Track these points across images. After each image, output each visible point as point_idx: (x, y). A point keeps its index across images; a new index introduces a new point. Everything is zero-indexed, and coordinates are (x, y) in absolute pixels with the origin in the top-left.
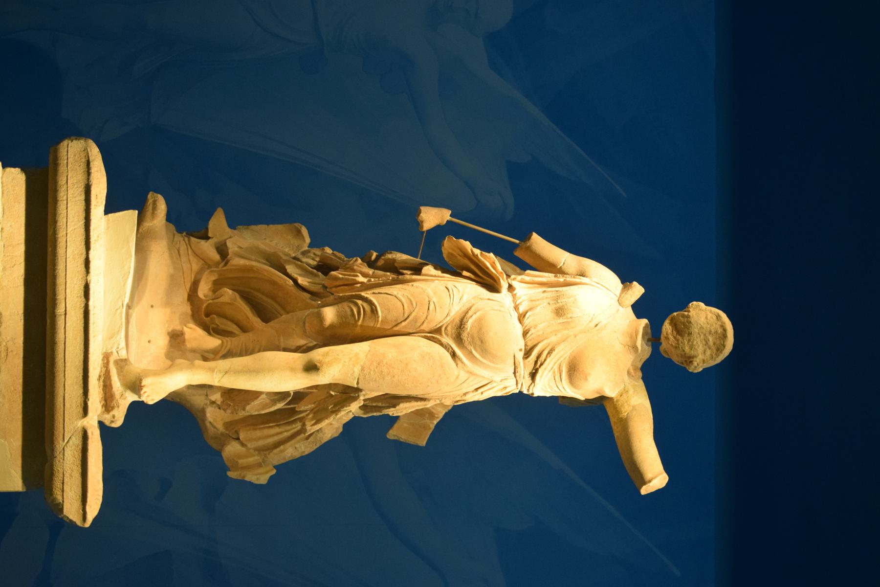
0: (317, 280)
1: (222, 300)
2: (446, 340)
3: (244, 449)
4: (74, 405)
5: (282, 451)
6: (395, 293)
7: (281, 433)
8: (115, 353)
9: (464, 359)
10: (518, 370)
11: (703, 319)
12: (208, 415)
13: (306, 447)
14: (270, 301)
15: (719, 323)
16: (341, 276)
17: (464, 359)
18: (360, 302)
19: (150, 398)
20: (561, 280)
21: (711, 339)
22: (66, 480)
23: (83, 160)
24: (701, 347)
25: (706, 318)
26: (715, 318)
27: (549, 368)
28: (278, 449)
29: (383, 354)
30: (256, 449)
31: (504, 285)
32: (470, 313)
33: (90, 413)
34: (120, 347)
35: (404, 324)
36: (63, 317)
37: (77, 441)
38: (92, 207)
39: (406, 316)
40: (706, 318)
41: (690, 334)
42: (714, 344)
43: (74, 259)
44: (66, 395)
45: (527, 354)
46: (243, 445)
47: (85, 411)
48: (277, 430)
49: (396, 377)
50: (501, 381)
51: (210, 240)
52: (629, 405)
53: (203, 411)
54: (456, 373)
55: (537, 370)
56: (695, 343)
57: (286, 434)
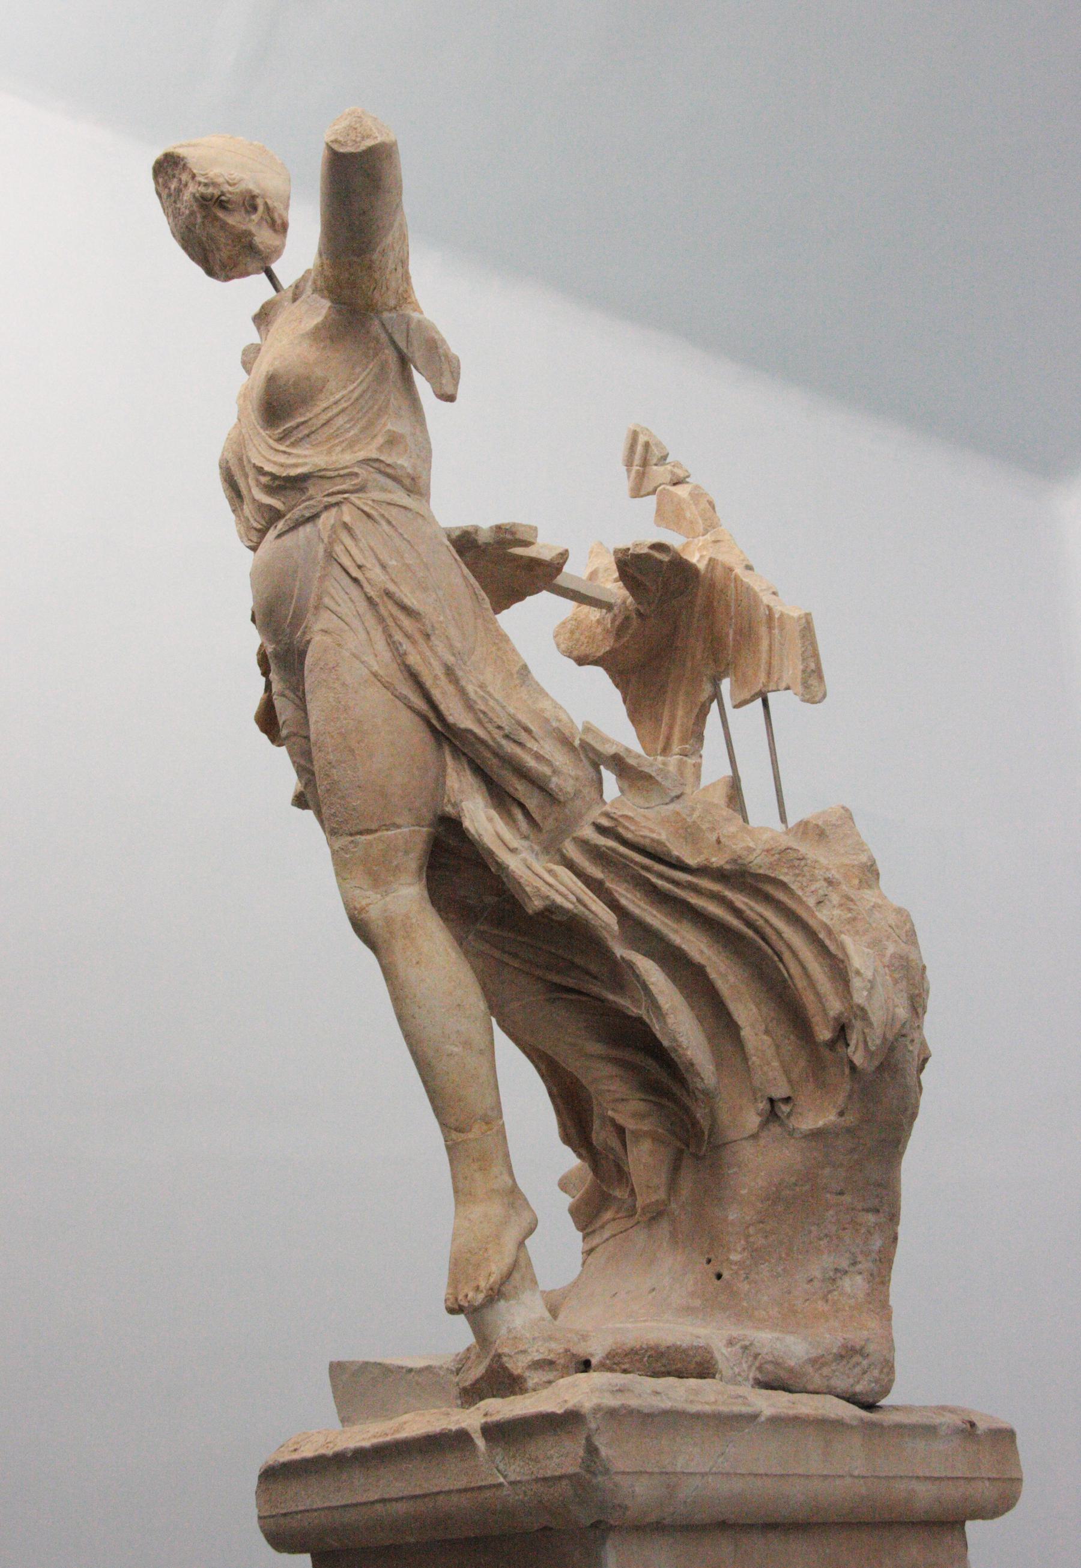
5: (830, 932)
7: (789, 947)
12: (821, 1123)
13: (813, 879)
19: (483, 1284)
27: (282, 459)
28: (827, 942)
33: (464, 1425)
42: (174, 176)
44: (459, 1485)
45: (275, 515)
47: (461, 1438)
48: (787, 956)
53: (816, 1135)
55: (288, 479)
57: (789, 932)
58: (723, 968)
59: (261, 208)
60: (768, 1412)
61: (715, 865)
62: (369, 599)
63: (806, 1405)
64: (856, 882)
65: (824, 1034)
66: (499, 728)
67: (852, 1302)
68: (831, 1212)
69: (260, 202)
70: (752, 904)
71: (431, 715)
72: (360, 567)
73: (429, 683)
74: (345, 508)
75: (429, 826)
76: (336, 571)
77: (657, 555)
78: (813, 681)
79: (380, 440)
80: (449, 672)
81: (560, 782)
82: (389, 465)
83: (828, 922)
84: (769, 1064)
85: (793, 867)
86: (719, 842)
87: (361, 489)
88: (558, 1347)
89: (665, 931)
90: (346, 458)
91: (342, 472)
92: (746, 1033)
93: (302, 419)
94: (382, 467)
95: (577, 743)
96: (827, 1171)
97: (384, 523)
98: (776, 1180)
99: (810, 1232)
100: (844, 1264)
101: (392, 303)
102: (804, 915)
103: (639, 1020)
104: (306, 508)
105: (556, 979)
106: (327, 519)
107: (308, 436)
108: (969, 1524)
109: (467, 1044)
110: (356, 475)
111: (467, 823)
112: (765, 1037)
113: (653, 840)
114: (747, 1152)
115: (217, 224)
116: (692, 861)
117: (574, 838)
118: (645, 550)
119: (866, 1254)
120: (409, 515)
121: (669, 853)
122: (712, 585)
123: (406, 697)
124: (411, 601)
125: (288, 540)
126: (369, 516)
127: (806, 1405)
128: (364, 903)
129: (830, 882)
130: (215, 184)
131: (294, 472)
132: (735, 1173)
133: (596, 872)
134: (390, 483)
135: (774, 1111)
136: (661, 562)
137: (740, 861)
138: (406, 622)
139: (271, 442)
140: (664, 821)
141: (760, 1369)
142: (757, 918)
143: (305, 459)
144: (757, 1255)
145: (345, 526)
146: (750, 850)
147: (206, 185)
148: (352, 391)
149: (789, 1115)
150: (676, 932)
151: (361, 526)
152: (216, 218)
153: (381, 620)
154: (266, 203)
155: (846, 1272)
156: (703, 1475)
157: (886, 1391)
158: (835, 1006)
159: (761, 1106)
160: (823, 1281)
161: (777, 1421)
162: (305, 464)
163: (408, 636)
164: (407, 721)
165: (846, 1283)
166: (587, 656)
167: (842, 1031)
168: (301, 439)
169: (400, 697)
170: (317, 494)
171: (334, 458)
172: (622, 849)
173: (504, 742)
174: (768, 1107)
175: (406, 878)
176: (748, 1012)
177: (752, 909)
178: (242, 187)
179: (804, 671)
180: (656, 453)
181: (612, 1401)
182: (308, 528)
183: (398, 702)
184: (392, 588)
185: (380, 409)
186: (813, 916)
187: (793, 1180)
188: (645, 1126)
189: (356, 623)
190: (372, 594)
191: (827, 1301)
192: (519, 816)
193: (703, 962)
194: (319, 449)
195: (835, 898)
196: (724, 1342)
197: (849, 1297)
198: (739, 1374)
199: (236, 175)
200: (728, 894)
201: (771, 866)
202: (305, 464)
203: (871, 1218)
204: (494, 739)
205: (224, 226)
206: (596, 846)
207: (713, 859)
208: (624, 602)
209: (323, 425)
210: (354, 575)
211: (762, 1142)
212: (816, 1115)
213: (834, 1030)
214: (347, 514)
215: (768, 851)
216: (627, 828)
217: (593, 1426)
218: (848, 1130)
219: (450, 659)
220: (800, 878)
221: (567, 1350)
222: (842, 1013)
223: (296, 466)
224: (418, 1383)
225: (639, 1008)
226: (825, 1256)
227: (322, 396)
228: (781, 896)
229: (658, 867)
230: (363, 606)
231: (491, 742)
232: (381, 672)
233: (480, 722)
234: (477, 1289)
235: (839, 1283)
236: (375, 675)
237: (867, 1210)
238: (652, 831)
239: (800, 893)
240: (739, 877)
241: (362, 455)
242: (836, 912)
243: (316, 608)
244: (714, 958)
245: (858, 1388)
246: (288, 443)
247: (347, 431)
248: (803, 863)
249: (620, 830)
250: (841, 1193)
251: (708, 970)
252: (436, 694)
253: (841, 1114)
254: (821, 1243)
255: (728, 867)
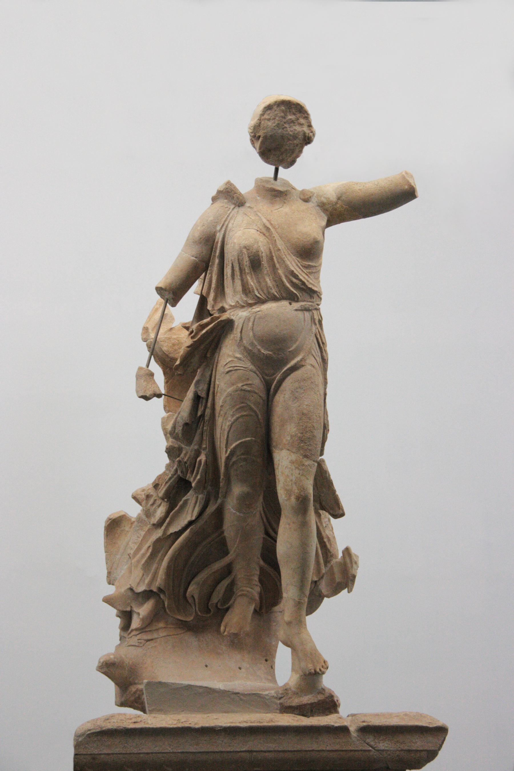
0: (191, 503)
1: (196, 597)
2: (278, 377)
3: (325, 576)
4: (338, 740)
6: (228, 423)
8: (281, 701)
9: (298, 358)
10: (307, 306)
11: (270, 124)
14: (199, 549)
15: (275, 107)
16: (198, 477)
17: (298, 358)
18: (234, 459)
20: (217, 261)
21: (290, 117)
22: (406, 748)
23: (99, 737)
24: (295, 127)
25: (269, 120)
26: (269, 112)
27: (306, 277)
28: (327, 544)
29: (292, 436)
30: (326, 565)
31: (225, 317)
32: (255, 351)
33: (345, 724)
34: (275, 695)
35: (260, 416)
36: (255, 754)
37: (370, 739)
38: (147, 726)
39: (253, 414)
40: (269, 120)
41: (282, 137)
42: (294, 114)
43: (197, 744)
44: (328, 748)
45: (292, 298)
46: (322, 578)
49: (315, 425)
50: (315, 324)
51: (135, 609)
52: (337, 203)
54: (309, 367)
56: (291, 133)
83: (330, 536)
104: (311, 306)
125: (300, 314)
139: (299, 265)
186: (324, 532)
223: (314, 285)
224: (241, 700)
246: (308, 271)
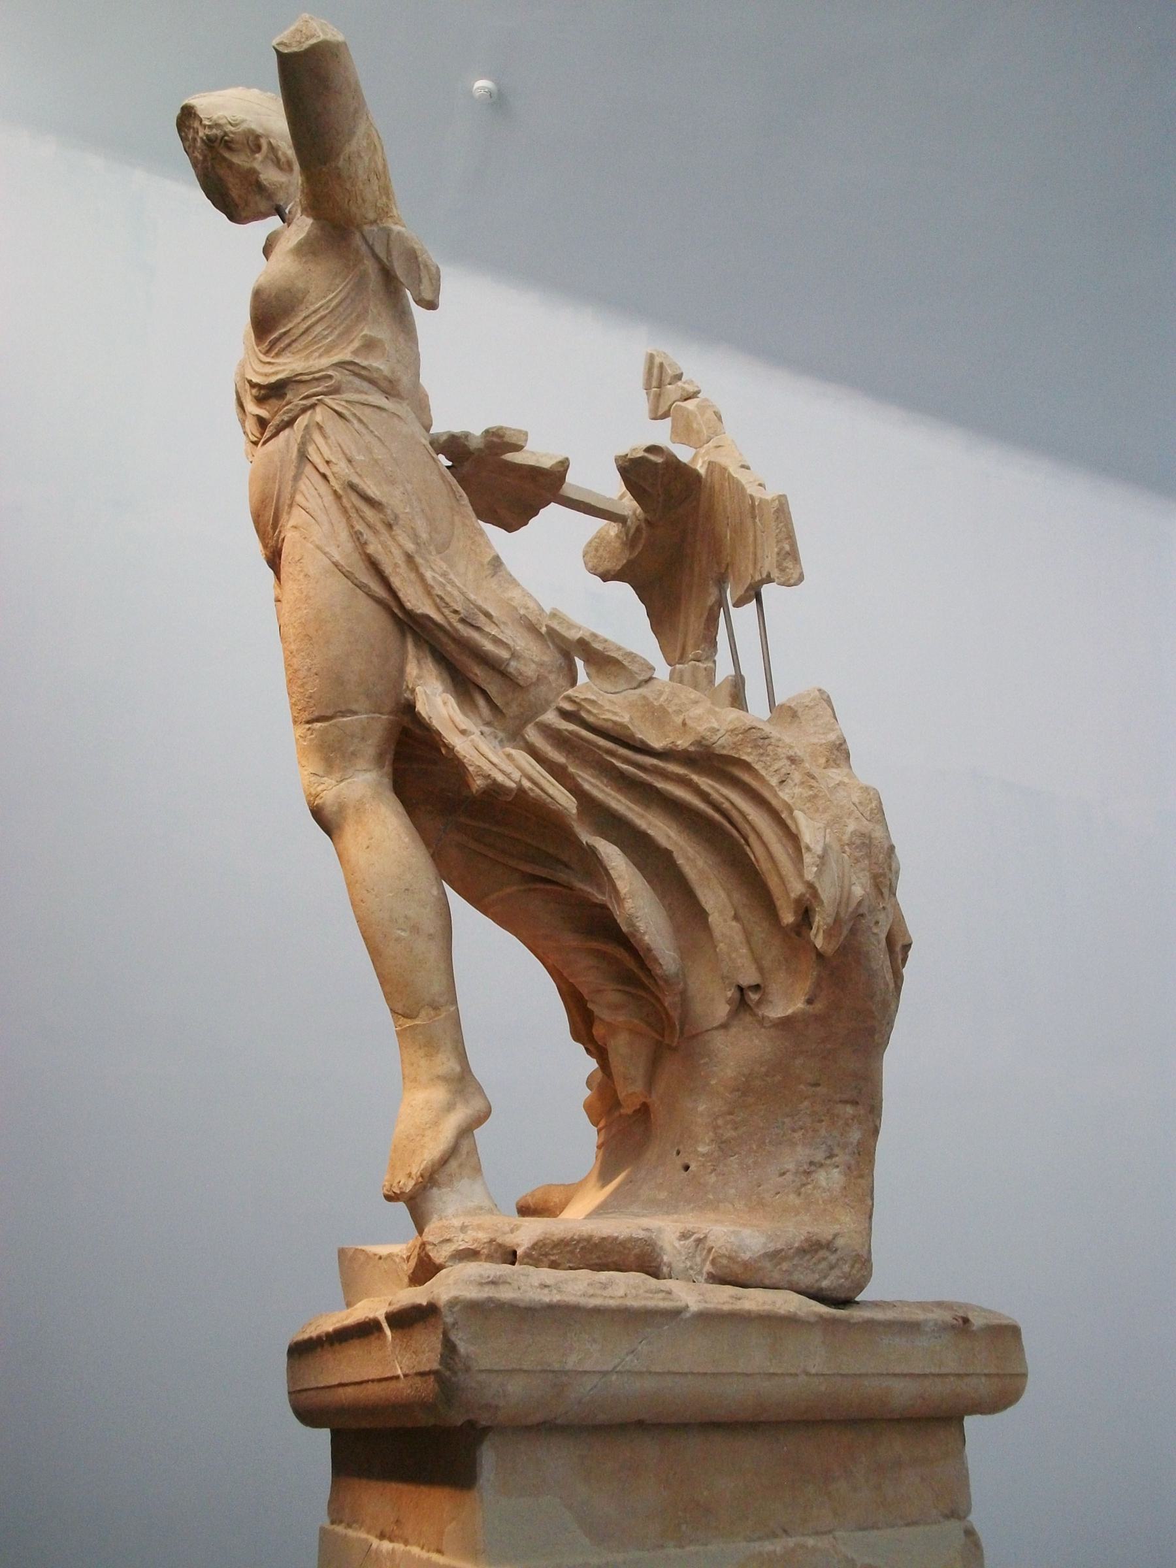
7: (754, 829)
12: (790, 1011)
13: (776, 758)
27: (268, 369)
48: (752, 838)
53: (786, 1023)
58: (691, 852)
59: (265, 147)
60: (694, 1307)
61: (680, 748)
62: (335, 492)
63: (754, 1300)
64: (822, 761)
65: (788, 918)
66: (456, 612)
67: (826, 1195)
68: (806, 1103)
69: (263, 142)
70: (717, 786)
71: (393, 604)
72: (328, 462)
73: (388, 570)
74: (318, 409)
75: (390, 713)
76: (308, 469)
77: (652, 457)
78: (788, 564)
79: (356, 344)
80: (409, 558)
81: (519, 666)
82: (364, 368)
83: (790, 802)
84: (737, 950)
85: (756, 746)
86: (684, 724)
87: (335, 391)
88: (483, 1236)
89: (630, 815)
90: (320, 362)
91: (317, 375)
92: (714, 919)
93: (283, 330)
94: (356, 369)
95: (544, 630)
96: (799, 1061)
97: (355, 422)
98: (746, 1071)
99: (783, 1123)
100: (819, 1156)
101: (371, 216)
102: (767, 794)
103: (604, 907)
105: (528, 868)
106: (302, 421)
107: (289, 345)
108: (969, 1422)
109: (415, 929)
110: (330, 377)
111: (420, 707)
112: (734, 923)
113: (615, 723)
114: (719, 1041)
115: (224, 164)
116: (657, 744)
117: (537, 724)
118: (641, 454)
119: (844, 1146)
120: (384, 414)
121: (632, 736)
122: (712, 488)
123: (366, 586)
124: (373, 491)
126: (340, 414)
127: (754, 1300)
128: (319, 789)
129: (792, 760)
130: (217, 125)
131: (273, 379)
132: (706, 1064)
133: (558, 757)
134: (365, 385)
135: (744, 1001)
136: (656, 464)
137: (704, 742)
138: (369, 513)
140: (632, 705)
141: (713, 1262)
142: (722, 800)
143: (287, 365)
144: (725, 1147)
145: (320, 427)
146: (714, 731)
147: (210, 127)
148: (331, 300)
149: (759, 1003)
150: (643, 816)
151: (333, 426)
152: (225, 159)
153: (345, 511)
154: (270, 143)
155: (821, 1165)
156: (605, 1374)
157: (860, 1288)
158: (797, 888)
159: (729, 994)
160: (797, 1173)
161: (708, 1318)
162: (284, 370)
163: (369, 526)
164: (366, 607)
165: (821, 1177)
166: (608, 572)
167: (805, 914)
168: (284, 349)
169: (360, 586)
170: (294, 398)
171: (311, 362)
172: (585, 733)
173: (460, 626)
174: (737, 995)
175: (361, 764)
176: (716, 896)
177: (717, 791)
178: (244, 126)
179: (778, 554)
180: (670, 372)
181: (473, 1293)
182: (287, 432)
183: (358, 590)
184: (356, 480)
185: (358, 316)
186: (776, 795)
187: (763, 1069)
188: (621, 1018)
189: (322, 518)
190: (337, 487)
191: (799, 1194)
192: (481, 702)
193: (670, 848)
194: (298, 357)
195: (797, 776)
196: (678, 1234)
197: (824, 1190)
198: (691, 1268)
199: (240, 116)
200: (695, 778)
201: (735, 746)
202: (284, 370)
203: (850, 1110)
204: (450, 624)
205: (231, 165)
206: (559, 731)
207: (679, 742)
208: (634, 513)
209: (304, 333)
210: (322, 470)
211: (733, 1030)
212: (787, 1002)
213: (796, 912)
214: (319, 415)
215: (732, 731)
216: (589, 712)
217: (449, 1320)
218: (817, 1018)
219: (410, 547)
220: (763, 758)
221: (492, 1241)
222: (802, 895)
223: (276, 373)
225: (604, 894)
226: (799, 1148)
227: (303, 307)
228: (746, 777)
229: (622, 751)
230: (329, 498)
231: (448, 628)
232: (342, 562)
233: (438, 609)
234: (410, 1175)
235: (814, 1176)
236: (336, 565)
237: (846, 1102)
238: (615, 714)
239: (763, 772)
240: (707, 759)
241: (336, 359)
242: (797, 790)
243: (291, 506)
244: (682, 843)
245: (825, 1284)
246: (273, 354)
247: (325, 337)
248: (767, 741)
249: (583, 714)
250: (817, 1085)
251: (675, 854)
252: (396, 582)
253: (810, 1002)
254: (796, 1135)
255: (692, 749)
